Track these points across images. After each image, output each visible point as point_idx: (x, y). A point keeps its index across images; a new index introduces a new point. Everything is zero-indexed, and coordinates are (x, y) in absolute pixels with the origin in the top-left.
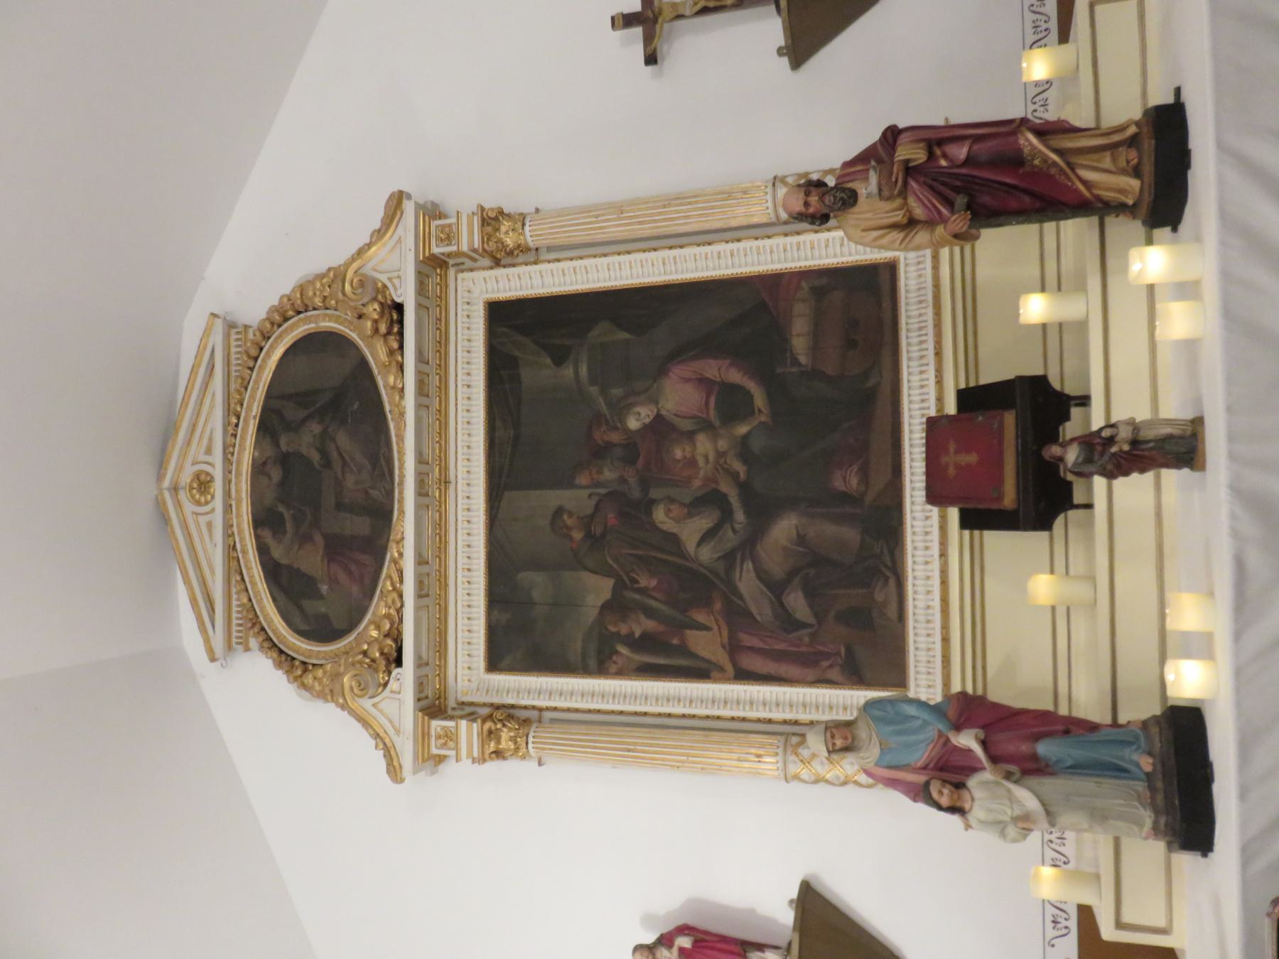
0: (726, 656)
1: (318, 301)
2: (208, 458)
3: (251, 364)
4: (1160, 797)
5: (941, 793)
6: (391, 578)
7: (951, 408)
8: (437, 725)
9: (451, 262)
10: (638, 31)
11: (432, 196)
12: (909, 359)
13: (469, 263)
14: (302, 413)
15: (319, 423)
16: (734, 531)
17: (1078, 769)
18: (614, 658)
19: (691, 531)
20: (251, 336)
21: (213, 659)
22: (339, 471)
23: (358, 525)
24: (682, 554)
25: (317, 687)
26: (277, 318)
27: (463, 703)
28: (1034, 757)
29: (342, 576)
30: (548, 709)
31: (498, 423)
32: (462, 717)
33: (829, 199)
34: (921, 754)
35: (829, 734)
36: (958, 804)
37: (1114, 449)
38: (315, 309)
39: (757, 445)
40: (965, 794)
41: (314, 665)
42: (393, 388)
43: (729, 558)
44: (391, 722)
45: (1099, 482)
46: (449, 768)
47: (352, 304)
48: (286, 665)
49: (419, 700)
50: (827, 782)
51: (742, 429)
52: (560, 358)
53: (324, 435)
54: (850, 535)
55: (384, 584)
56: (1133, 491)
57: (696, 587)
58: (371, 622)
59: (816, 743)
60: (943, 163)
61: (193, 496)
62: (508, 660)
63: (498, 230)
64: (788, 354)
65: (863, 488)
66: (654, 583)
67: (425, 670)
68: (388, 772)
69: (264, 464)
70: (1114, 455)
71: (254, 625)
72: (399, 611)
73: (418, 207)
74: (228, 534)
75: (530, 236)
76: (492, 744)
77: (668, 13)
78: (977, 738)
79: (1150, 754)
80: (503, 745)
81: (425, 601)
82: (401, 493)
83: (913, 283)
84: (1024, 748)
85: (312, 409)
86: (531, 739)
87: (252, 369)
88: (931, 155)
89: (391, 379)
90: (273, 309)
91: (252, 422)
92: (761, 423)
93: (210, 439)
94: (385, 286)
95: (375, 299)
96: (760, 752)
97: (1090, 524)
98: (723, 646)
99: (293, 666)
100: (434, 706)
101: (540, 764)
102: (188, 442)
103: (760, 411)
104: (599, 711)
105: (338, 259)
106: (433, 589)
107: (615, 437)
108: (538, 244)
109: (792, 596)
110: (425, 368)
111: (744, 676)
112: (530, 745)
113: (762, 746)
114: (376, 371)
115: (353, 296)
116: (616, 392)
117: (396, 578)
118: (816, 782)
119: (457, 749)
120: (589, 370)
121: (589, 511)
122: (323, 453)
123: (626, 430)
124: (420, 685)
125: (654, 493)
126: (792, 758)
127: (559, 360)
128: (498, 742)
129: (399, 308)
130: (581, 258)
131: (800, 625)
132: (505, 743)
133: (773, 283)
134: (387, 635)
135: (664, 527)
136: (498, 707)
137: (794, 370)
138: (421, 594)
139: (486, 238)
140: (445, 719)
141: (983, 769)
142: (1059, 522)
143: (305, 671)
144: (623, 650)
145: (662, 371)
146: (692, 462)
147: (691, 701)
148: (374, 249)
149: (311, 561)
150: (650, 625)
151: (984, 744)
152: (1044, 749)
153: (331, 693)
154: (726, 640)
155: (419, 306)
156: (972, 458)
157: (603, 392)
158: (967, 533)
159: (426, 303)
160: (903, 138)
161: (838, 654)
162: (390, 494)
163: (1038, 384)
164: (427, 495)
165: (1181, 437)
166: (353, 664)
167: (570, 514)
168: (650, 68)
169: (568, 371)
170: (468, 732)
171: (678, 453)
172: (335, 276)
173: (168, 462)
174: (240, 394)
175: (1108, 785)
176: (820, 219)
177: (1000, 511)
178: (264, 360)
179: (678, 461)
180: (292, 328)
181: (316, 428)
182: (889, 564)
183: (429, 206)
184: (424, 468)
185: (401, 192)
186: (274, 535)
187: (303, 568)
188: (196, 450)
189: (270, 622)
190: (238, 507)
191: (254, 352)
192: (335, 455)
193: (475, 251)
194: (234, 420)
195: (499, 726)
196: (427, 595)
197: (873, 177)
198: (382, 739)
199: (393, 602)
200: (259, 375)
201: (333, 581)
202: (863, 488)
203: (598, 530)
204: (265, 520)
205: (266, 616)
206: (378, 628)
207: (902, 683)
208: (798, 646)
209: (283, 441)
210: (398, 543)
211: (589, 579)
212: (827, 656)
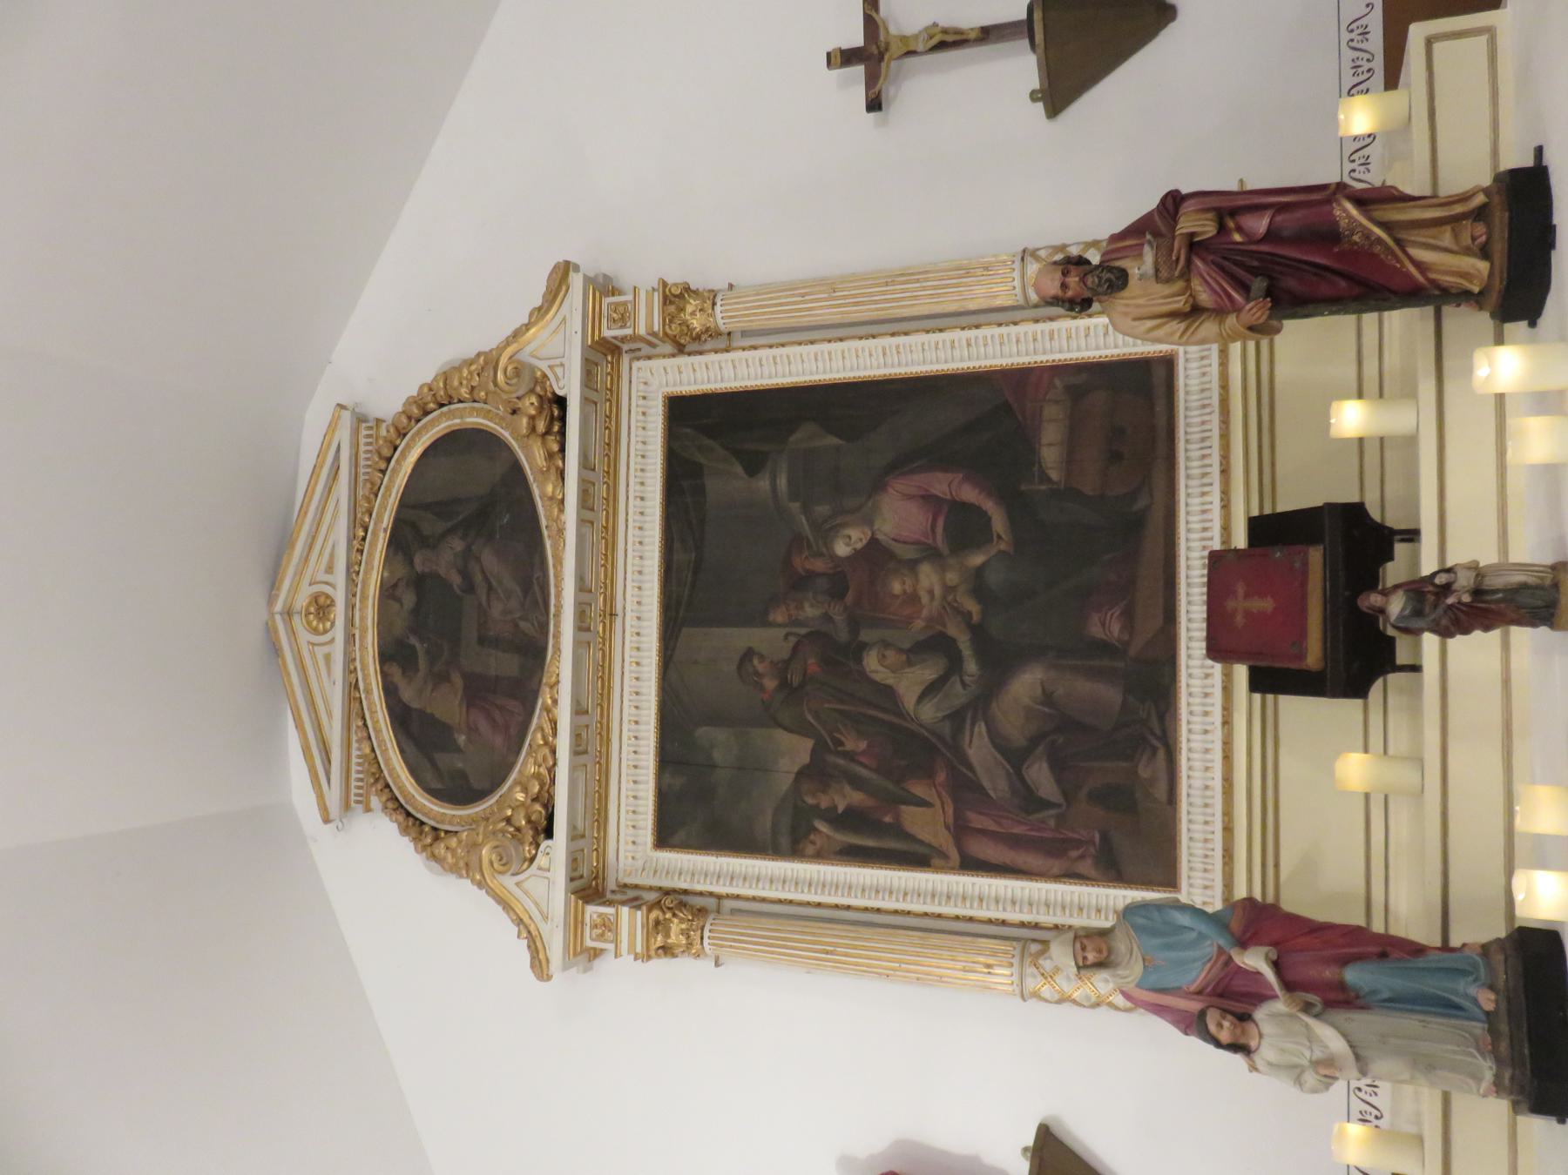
0: (951, 840)
1: (464, 392)
2: (327, 578)
3: (383, 466)
4: (1504, 1046)
5: (1220, 1026)
6: (542, 730)
7: (1240, 540)
8: (593, 911)
9: (625, 347)
10: (859, 70)
11: (606, 268)
12: (1188, 477)
13: (646, 350)
14: (441, 526)
15: (463, 538)
16: (964, 684)
17: (1399, 1002)
18: (812, 837)
19: (910, 683)
20: (383, 433)
21: (327, 820)
22: (484, 598)
23: (504, 664)
24: (899, 712)
25: (450, 859)
26: (416, 411)
27: (625, 886)
28: (1342, 986)
29: (483, 726)
30: (728, 896)
31: (677, 545)
32: (623, 903)
33: (1091, 280)
34: (1196, 974)
35: (1078, 945)
36: (1242, 1041)
37: (1450, 600)
38: (460, 401)
39: (994, 578)
40: (1251, 1027)
41: (447, 832)
42: (551, 498)
43: (956, 718)
44: (537, 904)
45: (1430, 641)
46: (606, 964)
47: (505, 397)
48: (414, 831)
49: (572, 879)
50: (1074, 1002)
51: (977, 559)
52: (753, 465)
53: (467, 554)
54: (1110, 694)
55: (534, 737)
56: (1475, 651)
57: (916, 753)
58: (516, 783)
59: (1061, 955)
60: (1237, 237)
61: (309, 623)
62: (681, 835)
63: (682, 310)
65: (1126, 637)
66: (863, 745)
67: (581, 843)
68: (532, 967)
69: (395, 586)
70: (1451, 607)
71: (377, 780)
72: (551, 770)
73: (588, 280)
74: (349, 670)
75: (721, 318)
76: (660, 938)
77: (896, 49)
78: (1267, 957)
79: (1492, 988)
80: (672, 940)
81: (583, 759)
82: (557, 625)
83: (1194, 384)
84: (1328, 973)
85: (449, 524)
86: (707, 934)
87: (383, 472)
88: (1222, 229)
89: (549, 489)
90: (411, 401)
91: (382, 535)
93: (332, 556)
94: (545, 376)
95: (532, 391)
96: (991, 961)
97: (1416, 692)
98: (947, 827)
99: (421, 832)
100: (589, 888)
101: (717, 964)
102: (306, 559)
103: (999, 537)
104: (791, 902)
105: (489, 342)
106: (593, 746)
107: (819, 565)
108: (730, 327)
109: (1036, 766)
110: (590, 476)
111: (972, 865)
112: (706, 941)
113: (994, 954)
114: (531, 478)
115: (507, 388)
116: (822, 509)
117: (548, 730)
118: (1059, 1002)
119: (616, 942)
120: (790, 482)
121: (785, 654)
122: (465, 574)
123: (833, 557)
124: (574, 861)
125: (866, 635)
126: (1031, 970)
127: (753, 469)
128: (667, 935)
129: (561, 402)
130: (783, 345)
131: (1047, 805)
132: (676, 938)
133: (1019, 380)
134: (535, 800)
135: (877, 677)
136: (667, 892)
137: (1043, 488)
138: (578, 750)
139: (669, 319)
140: (603, 904)
141: (1275, 997)
142: (1376, 690)
143: (437, 839)
144: (823, 827)
145: (879, 486)
146: (912, 598)
147: (906, 894)
148: (532, 331)
149: (447, 705)
150: (856, 797)
151: (1276, 965)
152: (1353, 975)
153: (466, 867)
154: (951, 820)
155: (586, 401)
156: (1265, 605)
157: (806, 509)
158: (1257, 697)
159: (593, 396)
160: (1187, 207)
161: (1092, 842)
162: (544, 628)
163: (1354, 513)
164: (588, 629)
165: (1537, 587)
166: (494, 833)
167: (762, 658)
168: (872, 115)
169: (763, 483)
170: (629, 921)
171: (897, 587)
172: (486, 363)
173: (282, 580)
174: (368, 500)
175: (1438, 1025)
176: (1080, 305)
177: (1300, 672)
178: (398, 461)
179: (897, 597)
180: (433, 423)
181: (458, 545)
182: (1158, 732)
183: (601, 280)
184: (586, 597)
185: (567, 263)
186: (404, 673)
187: (438, 715)
188: (316, 567)
189: (397, 778)
190: (362, 638)
191: (386, 452)
192: (478, 578)
193: (654, 334)
194: (361, 533)
195: (668, 915)
196: (585, 752)
197: (1149, 255)
198: (526, 927)
199: (545, 759)
200: (391, 480)
201: (472, 730)
202: (1126, 637)
203: (796, 680)
204: (394, 654)
205: (392, 771)
206: (525, 790)
207: (1171, 882)
208: (1039, 830)
209: (418, 560)
210: (551, 687)
211: (784, 739)
212: (1078, 844)
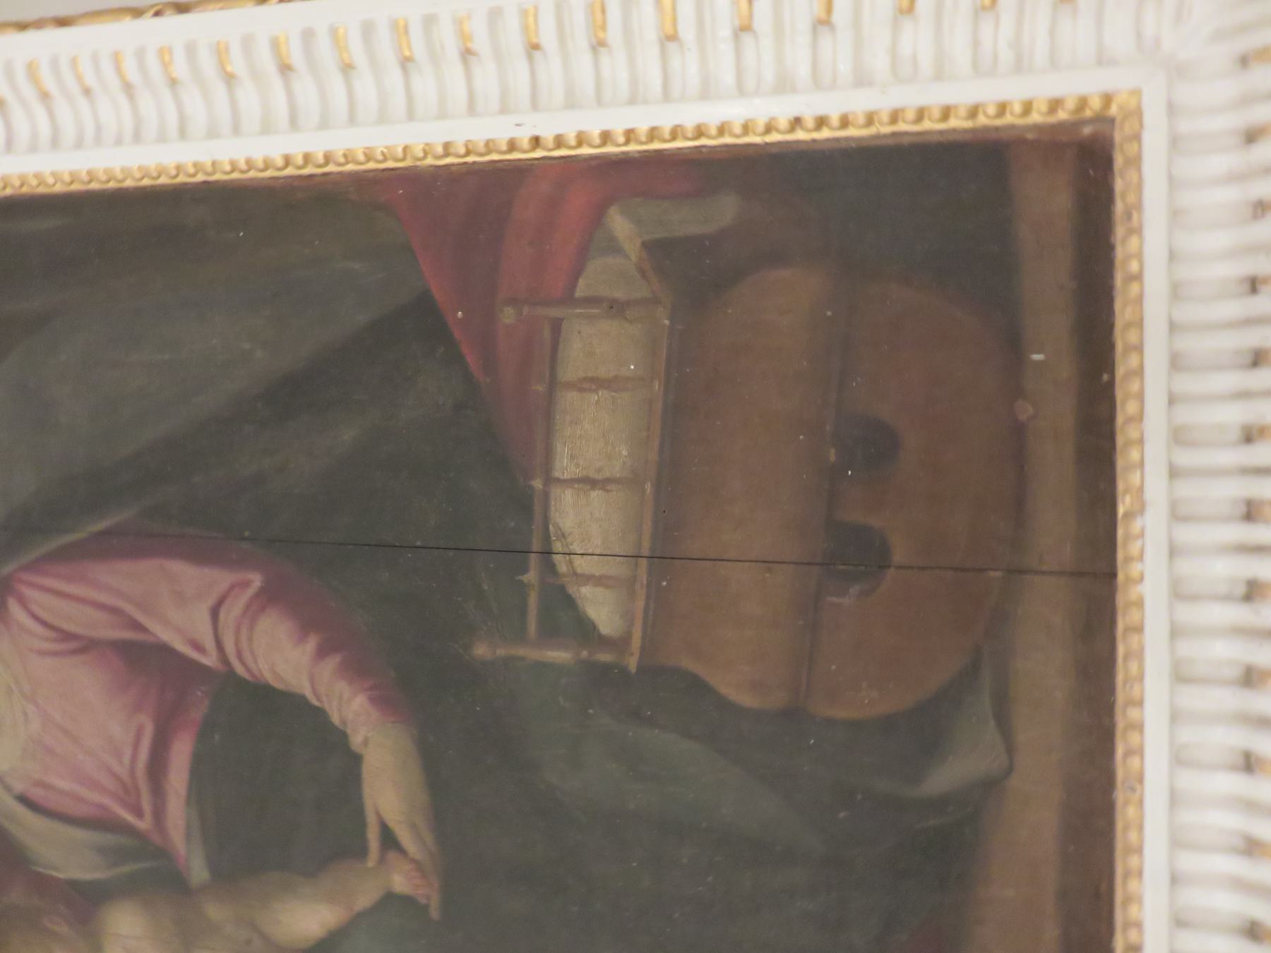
12: (1181, 676)
64: (531, 577)
92: (390, 899)
103: (389, 840)
137: (559, 655)
